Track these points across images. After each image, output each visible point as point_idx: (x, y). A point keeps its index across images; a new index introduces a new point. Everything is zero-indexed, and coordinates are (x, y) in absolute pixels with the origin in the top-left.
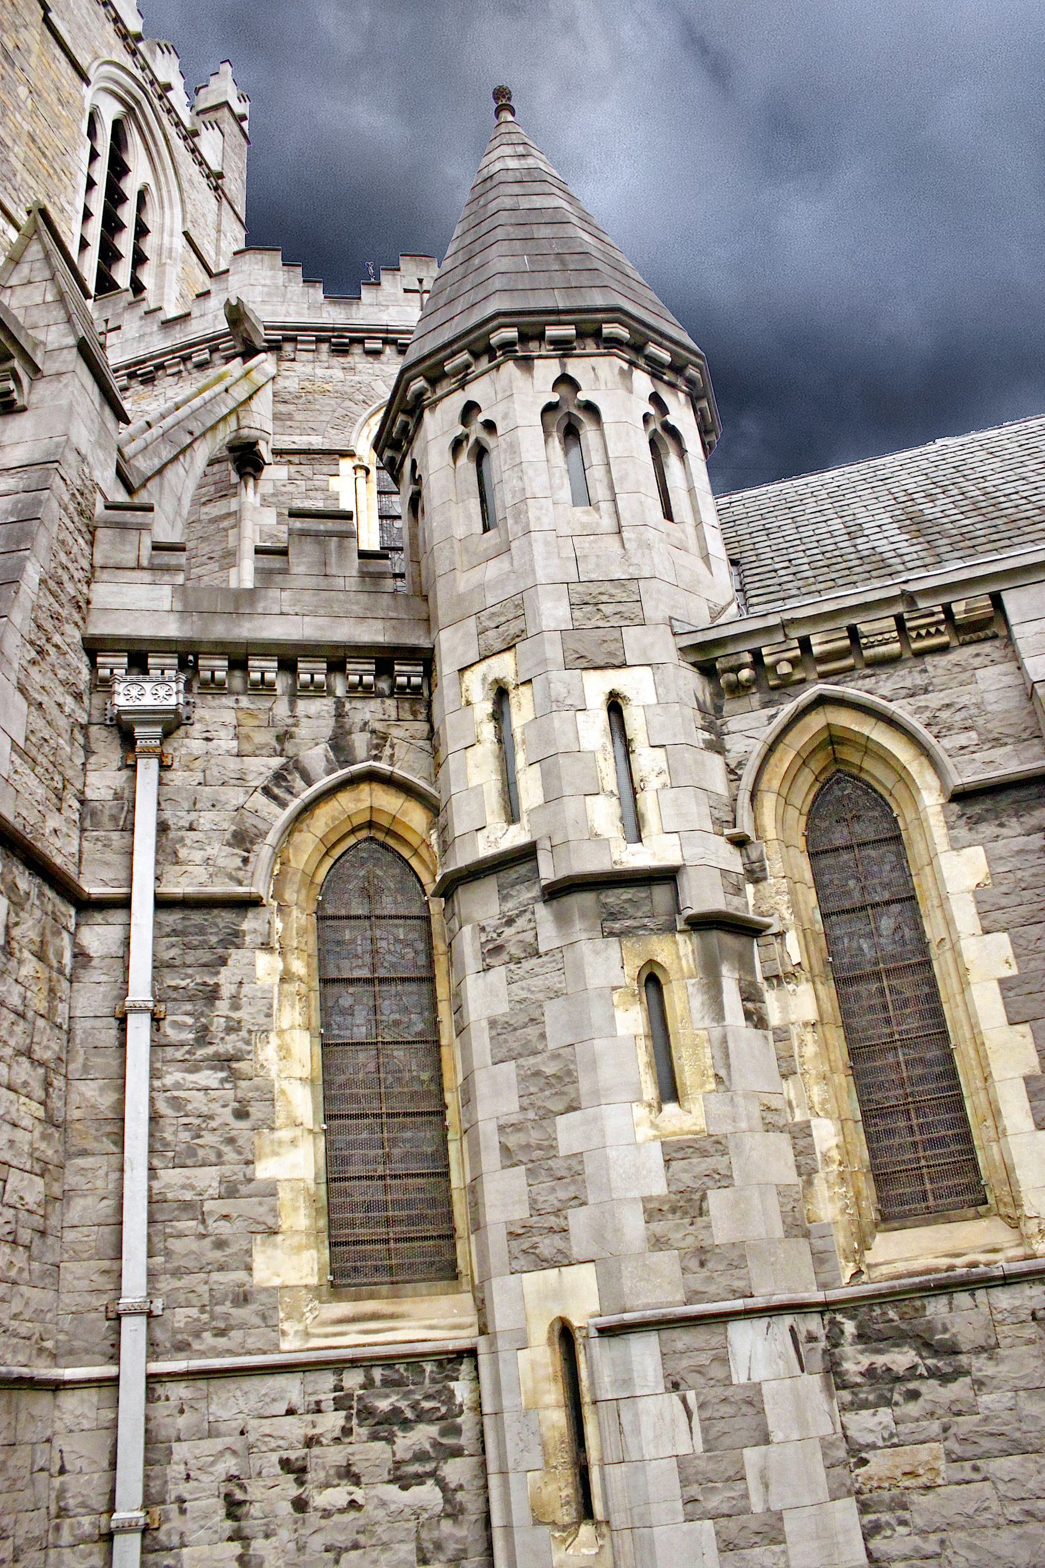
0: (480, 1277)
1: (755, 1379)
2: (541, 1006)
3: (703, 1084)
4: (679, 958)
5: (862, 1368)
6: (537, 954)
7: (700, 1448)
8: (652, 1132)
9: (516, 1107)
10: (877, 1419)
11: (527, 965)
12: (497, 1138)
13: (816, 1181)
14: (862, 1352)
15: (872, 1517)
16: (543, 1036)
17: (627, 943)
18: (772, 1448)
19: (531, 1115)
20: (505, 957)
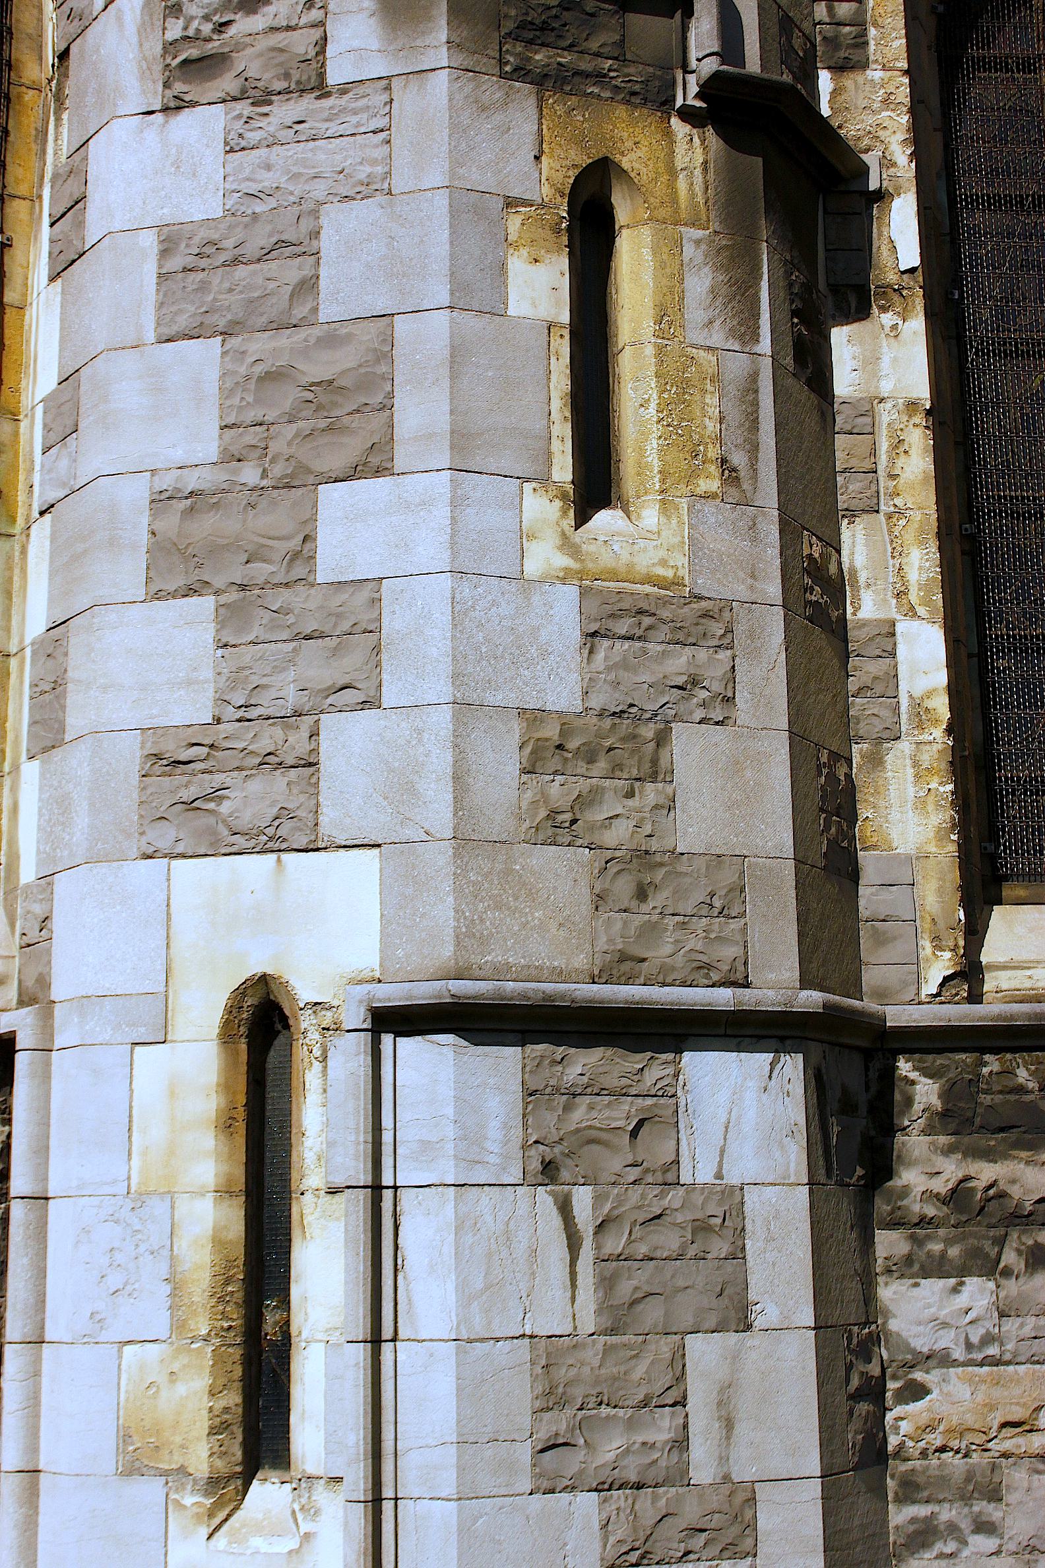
0: (43, 857)
1: (733, 1178)
2: (315, 213)
3: (692, 476)
4: (672, 172)
5: (941, 1186)
6: (320, 89)
7: (588, 1322)
8: (562, 561)
9: (208, 447)
10: (962, 1300)
11: (284, 112)
12: (145, 520)
13: (889, 759)
14: (948, 1151)
15: (922, 1511)
16: (308, 286)
17: (557, 105)
18: (751, 1340)
19: (250, 475)
20: (227, 83)
